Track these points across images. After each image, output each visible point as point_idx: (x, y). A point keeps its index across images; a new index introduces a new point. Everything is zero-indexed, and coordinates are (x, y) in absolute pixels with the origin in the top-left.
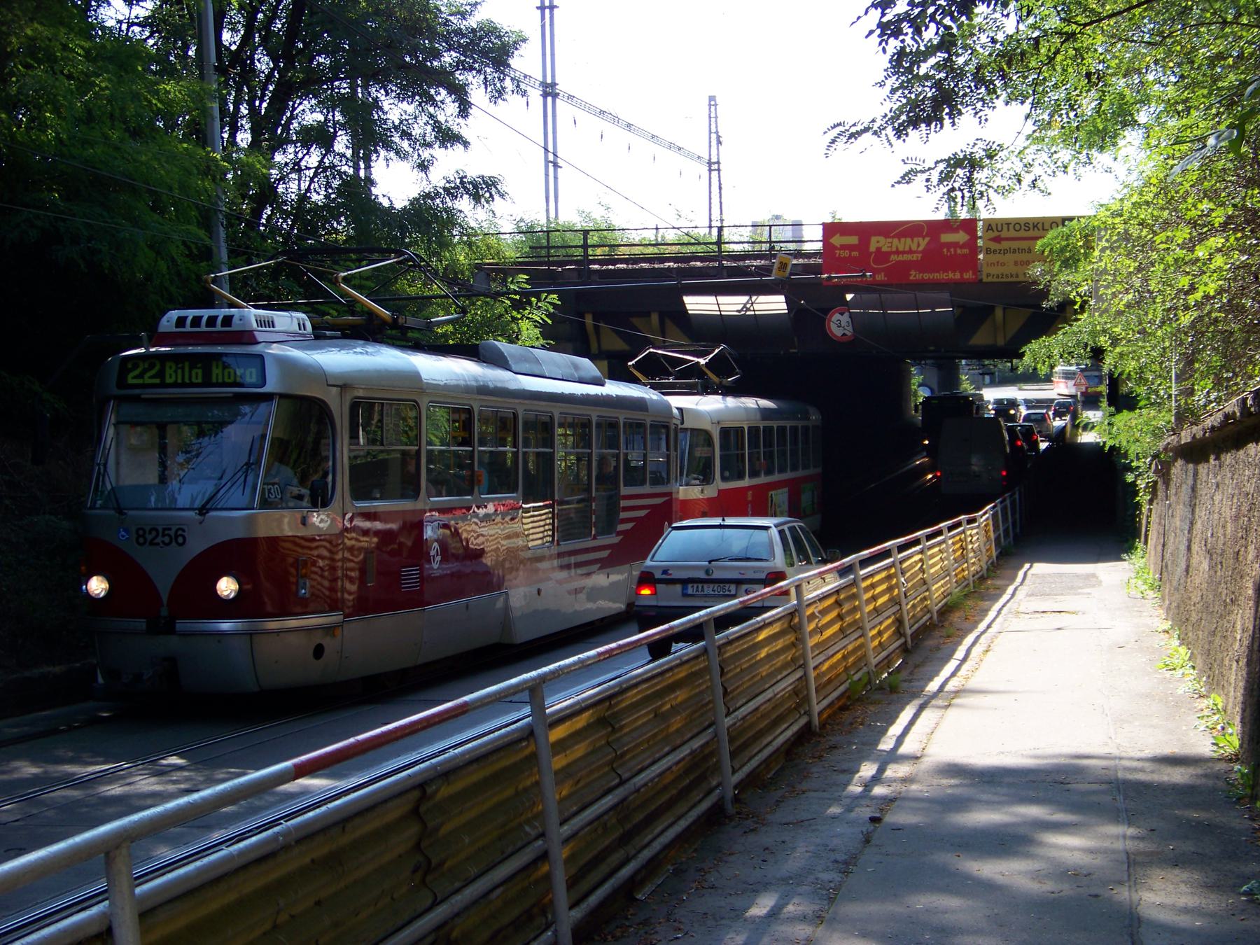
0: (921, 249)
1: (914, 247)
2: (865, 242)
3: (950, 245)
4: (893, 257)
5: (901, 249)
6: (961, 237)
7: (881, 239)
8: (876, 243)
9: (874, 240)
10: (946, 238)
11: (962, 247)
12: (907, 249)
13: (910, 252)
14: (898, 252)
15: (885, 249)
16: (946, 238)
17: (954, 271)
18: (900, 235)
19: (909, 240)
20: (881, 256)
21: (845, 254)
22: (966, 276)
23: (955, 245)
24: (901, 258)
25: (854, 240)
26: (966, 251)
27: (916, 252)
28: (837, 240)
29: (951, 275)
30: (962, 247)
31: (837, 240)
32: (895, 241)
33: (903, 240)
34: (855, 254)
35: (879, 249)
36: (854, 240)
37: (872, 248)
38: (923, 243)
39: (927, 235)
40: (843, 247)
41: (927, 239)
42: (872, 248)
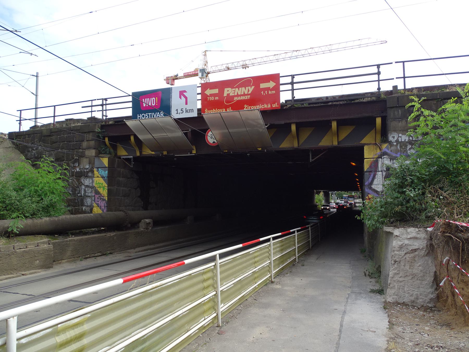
0: (250, 92)
1: (246, 93)
2: (222, 91)
3: (264, 89)
4: (236, 99)
5: (239, 94)
6: (271, 84)
7: (230, 89)
8: (228, 91)
9: (226, 90)
10: (263, 86)
11: (272, 90)
12: (242, 93)
13: (244, 95)
14: (238, 96)
15: (231, 94)
16: (263, 86)
17: (267, 104)
18: (238, 87)
19: (243, 88)
20: (230, 99)
21: (212, 99)
22: (274, 106)
23: (268, 89)
24: (239, 98)
25: (216, 91)
26: (274, 92)
27: (248, 95)
28: (208, 92)
29: (266, 106)
30: (272, 90)
31: (208, 92)
32: (237, 89)
33: (240, 89)
34: (217, 98)
35: (228, 95)
36: (216, 91)
37: (225, 95)
38: (251, 89)
39: (253, 85)
40: (211, 95)
41: (253, 87)
42: (225, 95)
